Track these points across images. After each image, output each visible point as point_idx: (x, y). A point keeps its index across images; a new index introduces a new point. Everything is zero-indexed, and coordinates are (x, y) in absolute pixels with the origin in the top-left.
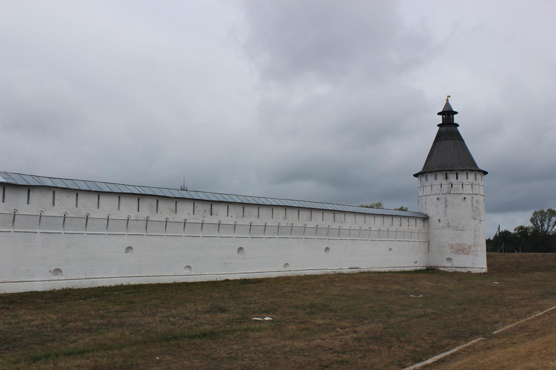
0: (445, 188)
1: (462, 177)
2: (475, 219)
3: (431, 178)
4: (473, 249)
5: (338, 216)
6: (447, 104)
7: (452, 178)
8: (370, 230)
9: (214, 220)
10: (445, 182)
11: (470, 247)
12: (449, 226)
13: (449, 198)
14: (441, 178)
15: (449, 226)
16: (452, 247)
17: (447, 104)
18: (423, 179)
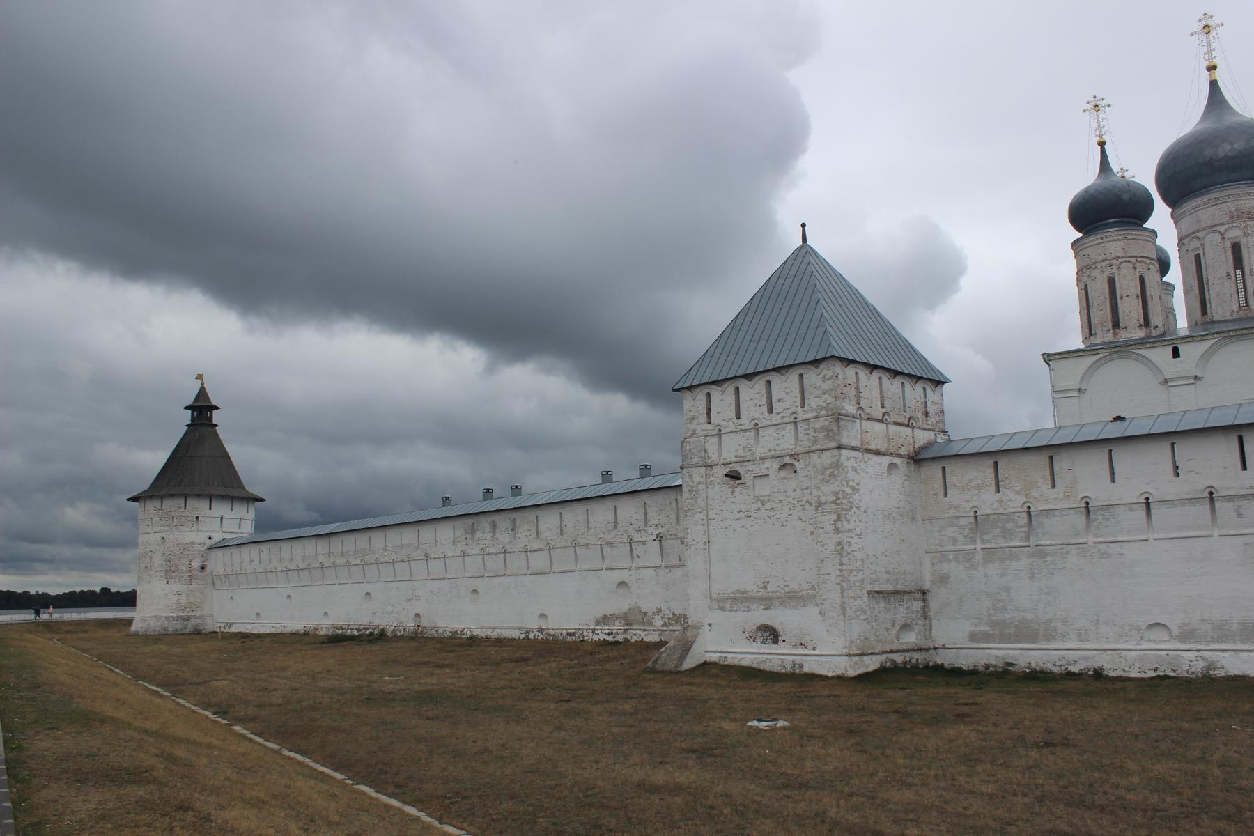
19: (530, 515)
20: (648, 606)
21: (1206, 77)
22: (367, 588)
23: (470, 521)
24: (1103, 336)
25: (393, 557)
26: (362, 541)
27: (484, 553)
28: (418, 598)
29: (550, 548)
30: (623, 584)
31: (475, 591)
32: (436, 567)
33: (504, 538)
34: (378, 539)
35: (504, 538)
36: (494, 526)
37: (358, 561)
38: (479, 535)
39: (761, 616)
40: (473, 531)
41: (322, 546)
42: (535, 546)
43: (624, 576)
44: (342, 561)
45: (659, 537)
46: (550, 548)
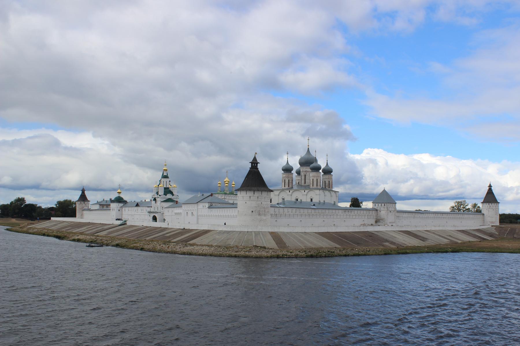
0: (489, 207)
1: (493, 204)
2: (496, 215)
3: (485, 204)
4: (495, 222)
5: (463, 215)
6: (490, 184)
7: (490, 204)
8: (470, 218)
9: (443, 217)
10: (489, 205)
11: (494, 222)
12: (489, 216)
13: (490, 210)
14: (487, 204)
15: (489, 216)
16: (490, 222)
17: (490, 184)
18: (483, 204)
19: (354, 210)
20: (366, 223)
21: (308, 147)
22: (324, 219)
23: (345, 210)
24: (319, 187)
25: (331, 214)
26: (323, 211)
27: (347, 215)
28: (334, 222)
29: (356, 215)
30: (364, 220)
31: (345, 221)
32: (339, 217)
33: (350, 213)
34: (327, 211)
35: (350, 213)
36: (348, 211)
37: (322, 214)
38: (346, 212)
39: (392, 224)
40: (345, 212)
41: (313, 211)
42: (354, 215)
43: (364, 219)
44: (319, 214)
45: (368, 215)
46: (356, 215)
